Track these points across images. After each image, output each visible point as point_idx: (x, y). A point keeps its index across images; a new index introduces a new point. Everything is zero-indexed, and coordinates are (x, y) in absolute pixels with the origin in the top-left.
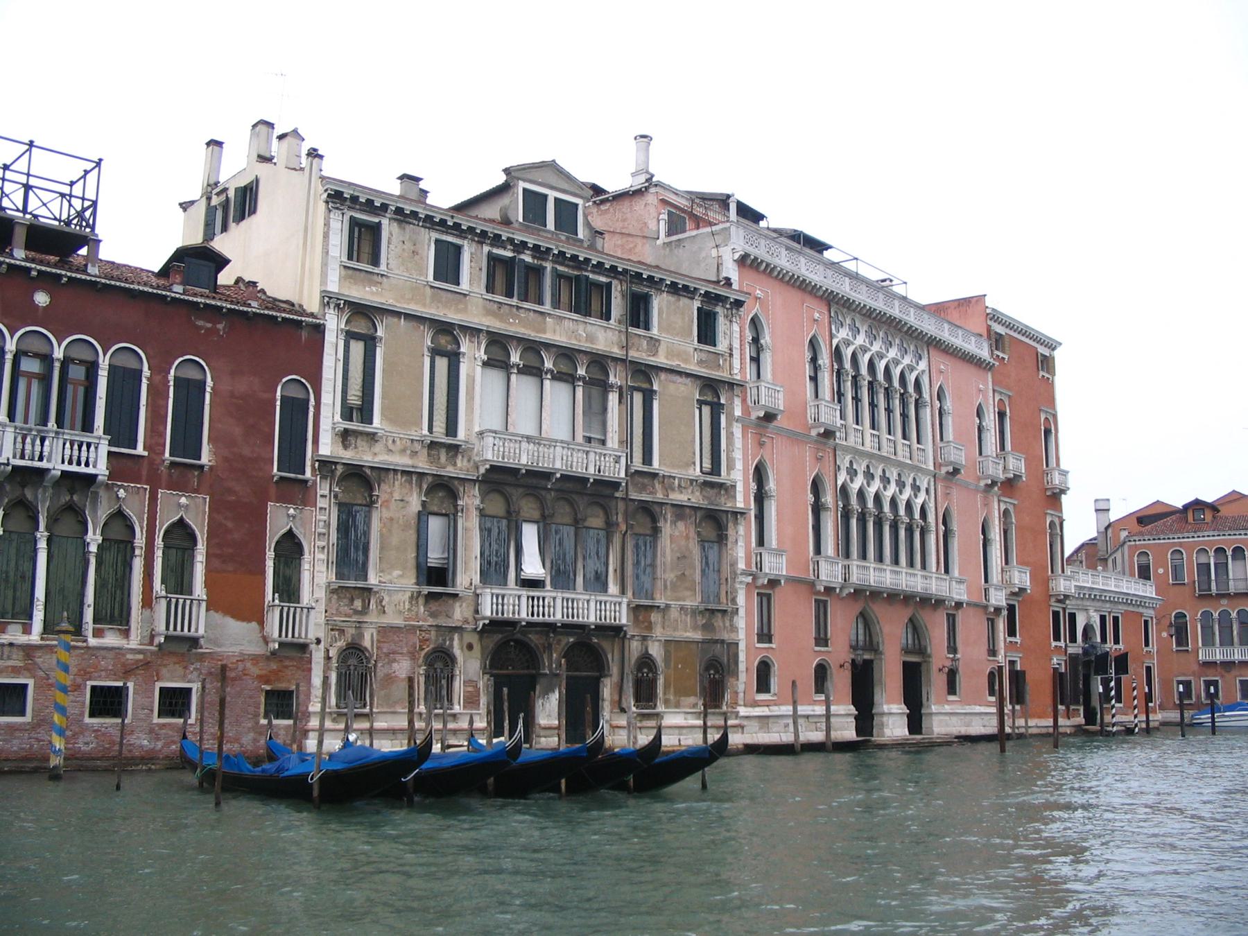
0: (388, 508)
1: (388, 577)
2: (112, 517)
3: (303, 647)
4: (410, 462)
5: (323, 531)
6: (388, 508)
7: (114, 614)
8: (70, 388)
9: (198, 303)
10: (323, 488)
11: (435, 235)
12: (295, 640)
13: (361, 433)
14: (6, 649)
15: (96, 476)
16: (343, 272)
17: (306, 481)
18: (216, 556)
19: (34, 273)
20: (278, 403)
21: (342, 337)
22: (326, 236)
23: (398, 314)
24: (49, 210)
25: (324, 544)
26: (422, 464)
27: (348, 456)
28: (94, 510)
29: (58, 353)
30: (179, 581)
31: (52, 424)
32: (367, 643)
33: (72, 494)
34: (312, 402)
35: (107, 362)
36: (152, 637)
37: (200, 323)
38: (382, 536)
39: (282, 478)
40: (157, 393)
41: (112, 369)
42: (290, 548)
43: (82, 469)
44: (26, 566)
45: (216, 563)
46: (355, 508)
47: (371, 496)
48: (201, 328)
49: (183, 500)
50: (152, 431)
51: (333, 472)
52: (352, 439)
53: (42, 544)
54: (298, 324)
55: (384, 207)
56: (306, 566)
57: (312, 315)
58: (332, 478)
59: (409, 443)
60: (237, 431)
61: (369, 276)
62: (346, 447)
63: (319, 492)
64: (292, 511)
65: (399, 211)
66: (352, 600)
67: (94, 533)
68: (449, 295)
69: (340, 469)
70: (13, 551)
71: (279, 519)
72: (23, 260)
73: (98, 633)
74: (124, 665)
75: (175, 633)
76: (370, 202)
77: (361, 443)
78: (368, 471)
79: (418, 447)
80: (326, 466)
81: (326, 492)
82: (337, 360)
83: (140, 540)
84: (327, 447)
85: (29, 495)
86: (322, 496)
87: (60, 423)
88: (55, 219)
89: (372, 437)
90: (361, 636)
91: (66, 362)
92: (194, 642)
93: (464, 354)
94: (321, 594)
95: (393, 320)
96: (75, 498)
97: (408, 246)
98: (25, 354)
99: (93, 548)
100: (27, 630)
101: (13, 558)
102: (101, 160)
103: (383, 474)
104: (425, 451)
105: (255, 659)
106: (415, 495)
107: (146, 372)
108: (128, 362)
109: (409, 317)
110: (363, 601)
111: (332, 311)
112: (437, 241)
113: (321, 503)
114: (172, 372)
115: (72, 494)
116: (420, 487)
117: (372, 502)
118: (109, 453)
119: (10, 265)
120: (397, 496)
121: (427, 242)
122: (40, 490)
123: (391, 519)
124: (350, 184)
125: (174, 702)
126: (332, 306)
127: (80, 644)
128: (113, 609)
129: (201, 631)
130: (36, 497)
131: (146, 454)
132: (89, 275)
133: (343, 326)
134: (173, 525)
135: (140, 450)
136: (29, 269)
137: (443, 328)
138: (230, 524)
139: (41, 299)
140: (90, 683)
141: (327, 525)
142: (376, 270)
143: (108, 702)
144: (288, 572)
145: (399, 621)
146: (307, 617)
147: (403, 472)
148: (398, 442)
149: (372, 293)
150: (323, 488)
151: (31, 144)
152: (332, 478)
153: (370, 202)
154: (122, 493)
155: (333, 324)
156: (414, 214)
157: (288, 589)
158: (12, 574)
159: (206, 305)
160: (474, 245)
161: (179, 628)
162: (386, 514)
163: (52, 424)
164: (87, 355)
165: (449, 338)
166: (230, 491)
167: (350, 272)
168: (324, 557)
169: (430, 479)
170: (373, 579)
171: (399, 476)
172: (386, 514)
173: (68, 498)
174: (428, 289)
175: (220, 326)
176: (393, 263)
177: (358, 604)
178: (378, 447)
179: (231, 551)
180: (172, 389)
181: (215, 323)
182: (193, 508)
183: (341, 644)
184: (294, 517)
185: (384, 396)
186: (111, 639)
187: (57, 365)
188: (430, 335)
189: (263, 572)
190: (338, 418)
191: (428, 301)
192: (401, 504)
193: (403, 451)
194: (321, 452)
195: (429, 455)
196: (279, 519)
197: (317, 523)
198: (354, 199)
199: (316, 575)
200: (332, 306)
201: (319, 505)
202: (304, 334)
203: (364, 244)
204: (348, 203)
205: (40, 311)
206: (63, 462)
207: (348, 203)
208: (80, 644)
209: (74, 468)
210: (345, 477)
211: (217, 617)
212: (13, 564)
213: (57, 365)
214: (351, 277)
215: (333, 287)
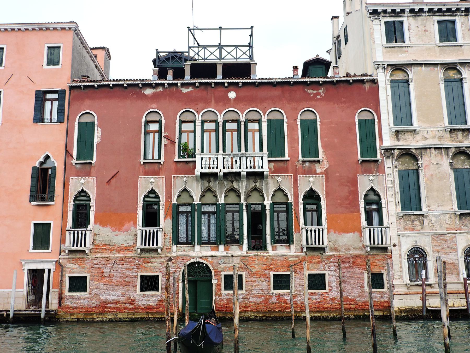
2: (276, 191)
3: (385, 249)
4: (439, 143)
5: (391, 186)
8: (250, 134)
9: (307, 82)
10: (388, 163)
11: (437, 18)
12: (380, 246)
13: (407, 131)
14: (231, 258)
15: (263, 172)
16: (385, 50)
17: (377, 161)
19: (226, 84)
20: (357, 123)
21: (389, 83)
22: (372, 34)
23: (421, 65)
24: (230, 56)
25: (393, 193)
26: (447, 142)
27: (402, 144)
28: (267, 190)
29: (243, 119)
31: (243, 151)
33: (255, 183)
35: (266, 118)
36: (302, 248)
37: (310, 91)
38: (427, 184)
39: (363, 161)
40: (292, 129)
41: (269, 121)
43: (257, 170)
47: (417, 164)
48: (311, 94)
49: (311, 179)
50: (292, 148)
51: (392, 154)
52: (401, 135)
54: (362, 81)
55: (403, 11)
57: (370, 76)
58: (393, 157)
59: (437, 132)
61: (400, 48)
62: (399, 140)
63: (386, 166)
65: (412, 11)
66: (413, 221)
67: (268, 200)
68: (451, 48)
69: (397, 152)
71: (364, 183)
72: (221, 79)
74: (288, 263)
75: (312, 246)
76: (394, 11)
77: (409, 136)
79: (441, 133)
80: (388, 151)
81: (390, 165)
82: (387, 96)
84: (388, 140)
85: (235, 185)
86: (388, 168)
87: (246, 150)
88: (235, 59)
89: (414, 132)
91: (246, 122)
92: (323, 249)
93: (465, 78)
94: (393, 219)
95: (418, 69)
96: (258, 184)
97: (421, 28)
98: (228, 121)
102: (252, 27)
103: (423, 151)
104: (448, 135)
106: (445, 159)
107: (286, 120)
108: (276, 116)
109: (426, 65)
110: (420, 221)
111: (381, 71)
112: (439, 22)
113: (387, 171)
114: (299, 118)
115: (255, 183)
116: (448, 155)
117: (419, 167)
118: (269, 161)
119: (215, 83)
120: (433, 161)
121: (432, 25)
122: (240, 183)
123: (432, 175)
124: (380, 4)
125: (317, 281)
126: (380, 68)
129: (326, 243)
130: (238, 186)
131: (289, 159)
132: (252, 79)
133: (388, 77)
134: (308, 192)
135: (287, 158)
136: (224, 83)
137: (450, 67)
139: (232, 95)
140: (272, 273)
142: (404, 45)
143: (282, 282)
146: (386, 232)
148: (430, 133)
150: (388, 163)
151: (220, 28)
152: (393, 157)
153: (394, 11)
154: (279, 179)
155: (383, 79)
156: (421, 10)
159: (311, 82)
160: (463, 17)
161: (314, 243)
162: (428, 173)
163: (243, 151)
164: (256, 117)
165: (455, 72)
167: (389, 49)
168: (393, 199)
169: (453, 150)
170: (425, 209)
171: (433, 151)
172: (428, 173)
173: (253, 185)
174: (437, 48)
175: (321, 91)
176: (413, 39)
178: (418, 137)
179: (339, 201)
180: (299, 126)
181: (317, 90)
184: (373, 180)
185: (418, 109)
186: (281, 250)
187: (243, 124)
188: (442, 71)
189: (359, 211)
190: (392, 125)
191: (438, 54)
192: (437, 166)
193: (434, 137)
194: (384, 145)
195: (451, 137)
196: (364, 183)
197: (388, 183)
198: (385, 11)
200: (380, 68)
201: (387, 172)
202: (367, 86)
203: (394, 33)
204: (382, 14)
205: (232, 101)
206: (247, 168)
207: (382, 14)
209: (252, 170)
210: (400, 156)
211: (334, 236)
213: (243, 124)
214: (389, 52)
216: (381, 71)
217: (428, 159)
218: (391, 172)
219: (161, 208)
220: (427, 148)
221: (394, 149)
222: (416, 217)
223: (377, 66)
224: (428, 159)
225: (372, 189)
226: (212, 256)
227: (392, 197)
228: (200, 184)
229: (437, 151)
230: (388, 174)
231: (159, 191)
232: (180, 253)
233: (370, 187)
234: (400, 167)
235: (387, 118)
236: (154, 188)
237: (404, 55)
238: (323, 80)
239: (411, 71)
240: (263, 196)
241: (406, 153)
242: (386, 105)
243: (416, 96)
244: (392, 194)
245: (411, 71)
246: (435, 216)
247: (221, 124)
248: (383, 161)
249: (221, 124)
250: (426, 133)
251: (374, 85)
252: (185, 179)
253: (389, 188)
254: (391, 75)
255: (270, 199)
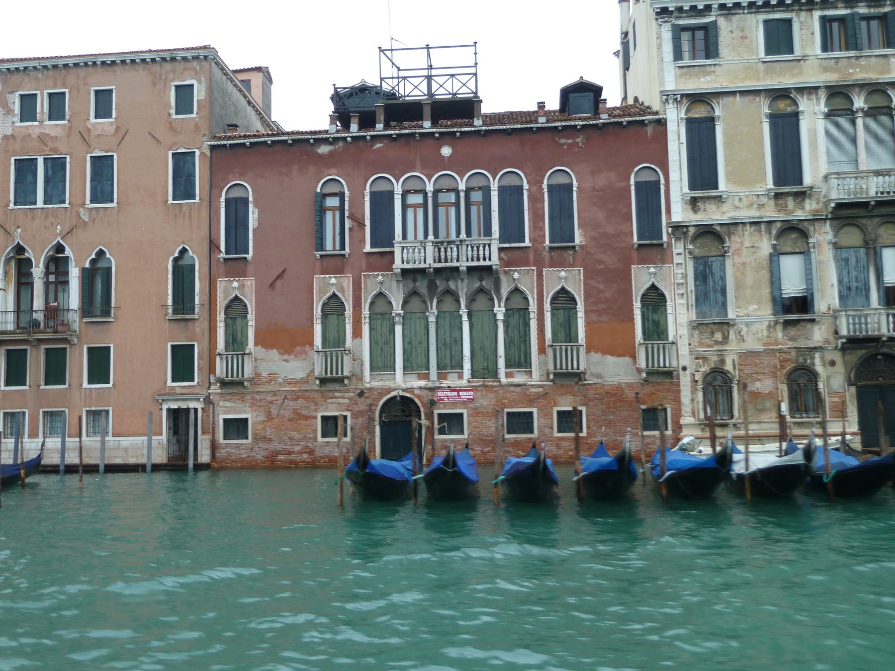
0: (739, 255)
1: (745, 312)
4: (758, 214)
6: (739, 255)
7: (519, 360)
9: (556, 127)
10: (678, 248)
13: (709, 198)
18: (592, 311)
30: (565, 330)
32: (729, 367)
34: (662, 181)
37: (563, 141)
42: (655, 299)
44: (456, 334)
45: (593, 317)
46: (710, 259)
48: (563, 145)
49: (563, 274)
53: (465, 318)
56: (669, 311)
59: (755, 198)
60: (601, 216)
63: (675, 251)
64: (652, 270)
66: (713, 333)
67: (500, 306)
69: (692, 230)
70: (447, 325)
71: (642, 277)
73: (508, 375)
78: (718, 228)
81: (681, 250)
83: (533, 307)
90: (723, 362)
94: (684, 331)
96: (484, 283)
99: (500, 316)
100: (461, 377)
101: (448, 328)
103: (732, 228)
105: (630, 385)
110: (723, 333)
111: (671, 106)
120: (747, 244)
123: (744, 264)
126: (671, 101)
127: (495, 384)
128: (519, 357)
138: (601, 287)
139: (446, 151)
141: (685, 276)
144: (656, 317)
145: (759, 347)
147: (752, 223)
149: (708, 82)
150: (678, 248)
157: (656, 330)
158: (448, 340)
166: (600, 262)
167: (685, 70)
168: (684, 301)
175: (579, 140)
177: (718, 336)
178: (726, 207)
179: (603, 306)
182: (572, 279)
183: (705, 369)
189: (632, 320)
190: (686, 189)
196: (642, 277)
197: (676, 275)
199: (680, 316)
201: (675, 261)
202: (650, 130)
208: (495, 384)
212: (448, 333)
214: (685, 74)
215: (670, 85)
216: (671, 106)
217: (739, 240)
218: (682, 261)
219: (347, 321)
220: (738, 223)
221: (687, 227)
222: (716, 327)
223: (665, 97)
224: (739, 240)
225: (653, 287)
226: (421, 388)
227: (682, 298)
228: (401, 285)
229: (753, 228)
230: (678, 264)
231: (344, 296)
232: (376, 384)
233: (651, 283)
234: (697, 252)
235: (678, 178)
236: (337, 293)
237: (708, 78)
238: (581, 123)
239: (718, 103)
240: (492, 300)
241: (707, 232)
242: (677, 158)
243: (725, 143)
244: (683, 295)
245: (718, 103)
246: (748, 325)
247: (430, 195)
248: (670, 244)
249: (430, 195)
250: (737, 200)
251: (662, 128)
252: (380, 277)
253: (678, 284)
254: (688, 111)
255: (503, 304)
